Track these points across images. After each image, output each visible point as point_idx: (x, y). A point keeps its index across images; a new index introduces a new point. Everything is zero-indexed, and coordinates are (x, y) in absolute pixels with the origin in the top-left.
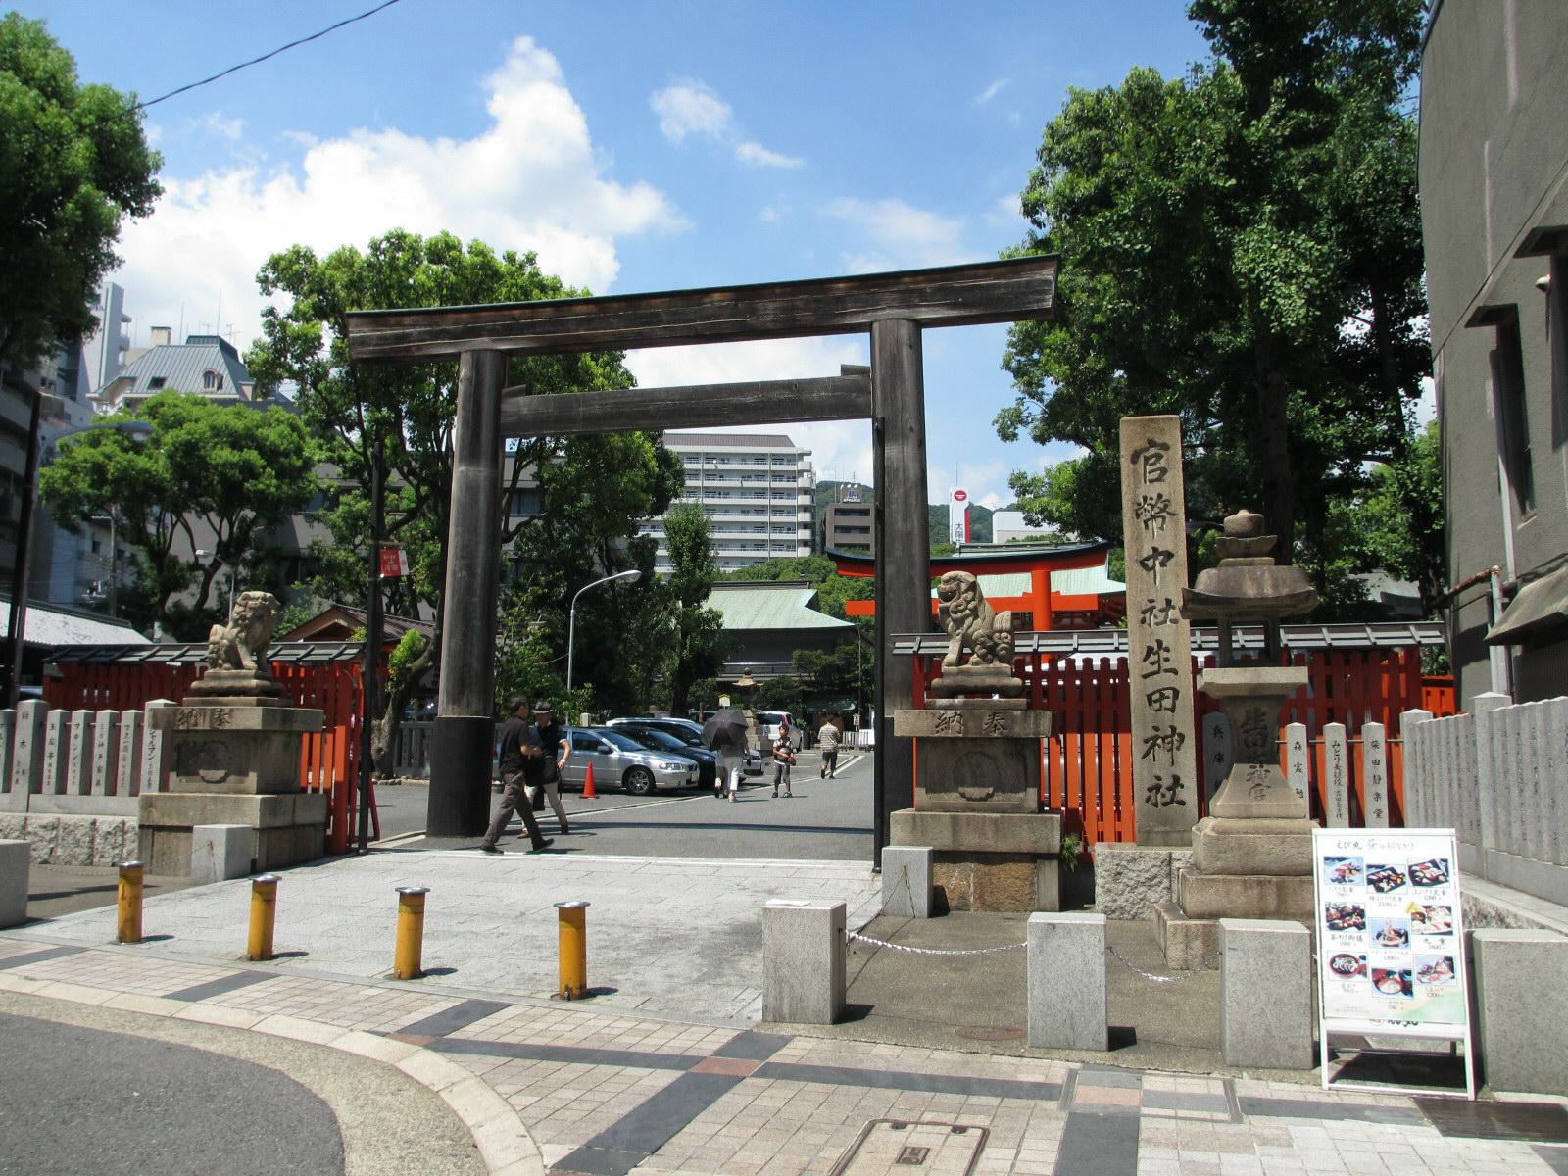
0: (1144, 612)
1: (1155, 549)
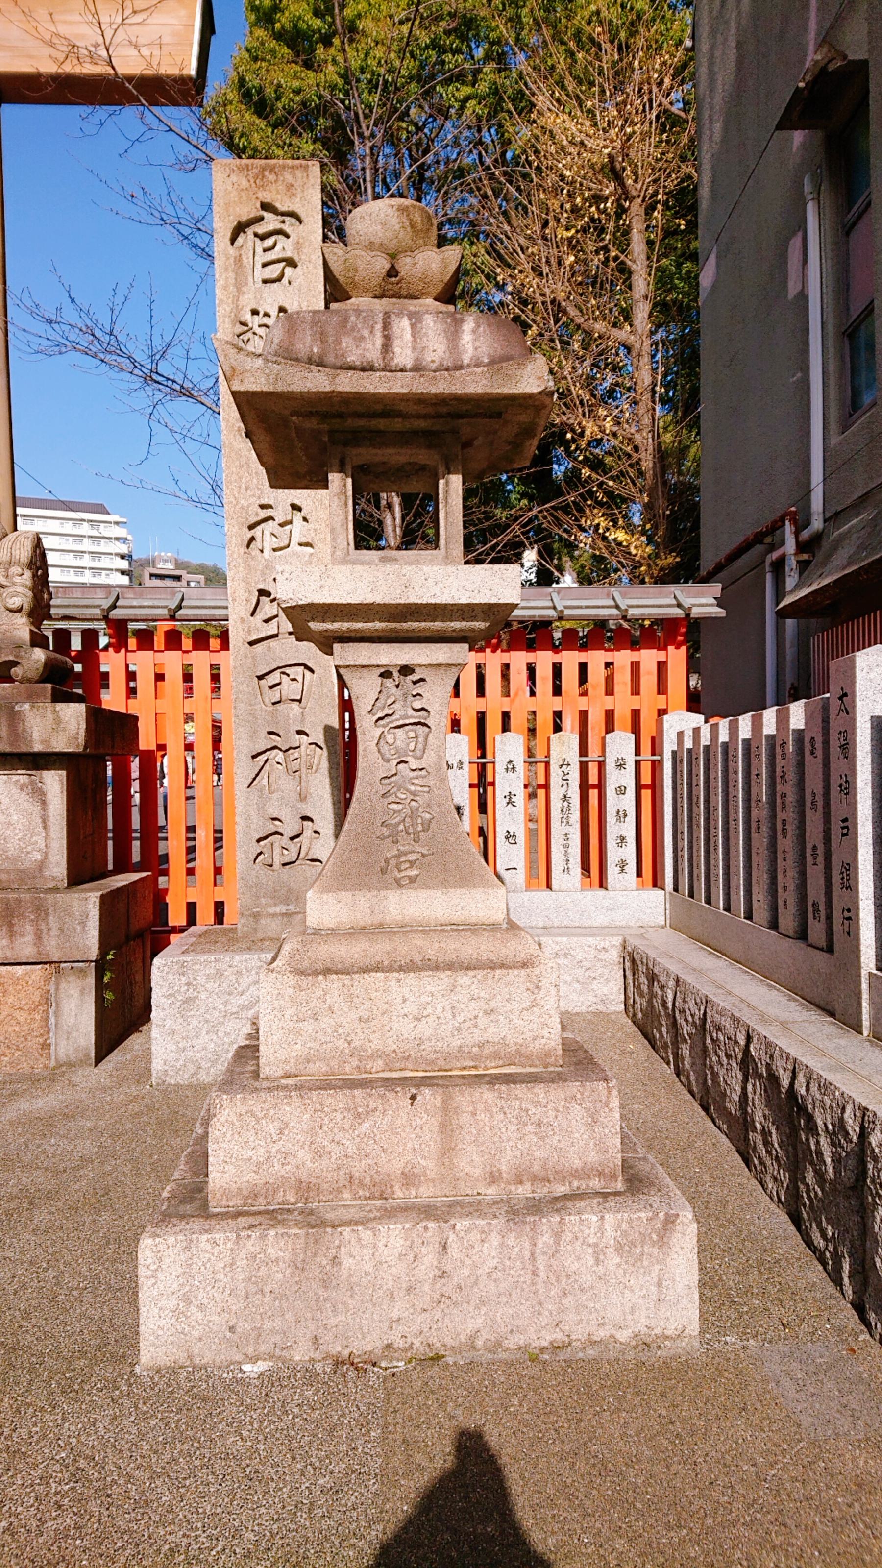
0: (251, 527)
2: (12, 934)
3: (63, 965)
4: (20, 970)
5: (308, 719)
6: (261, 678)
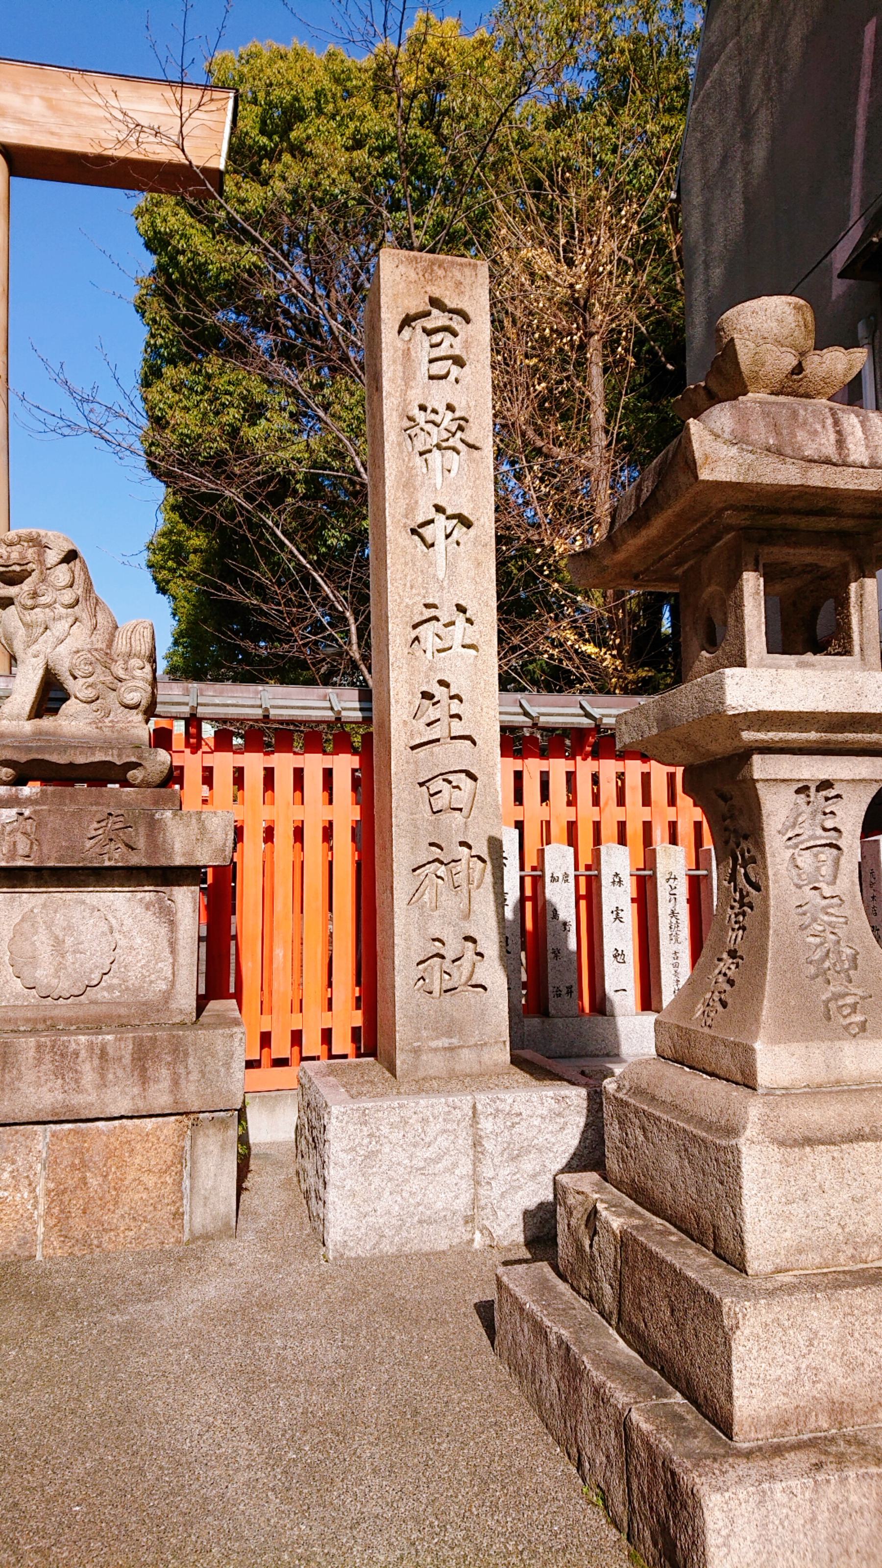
1: (439, 509)
2: (144, 1080)
3: (201, 1116)
4: (149, 1123)
5: (472, 829)
6: (421, 784)
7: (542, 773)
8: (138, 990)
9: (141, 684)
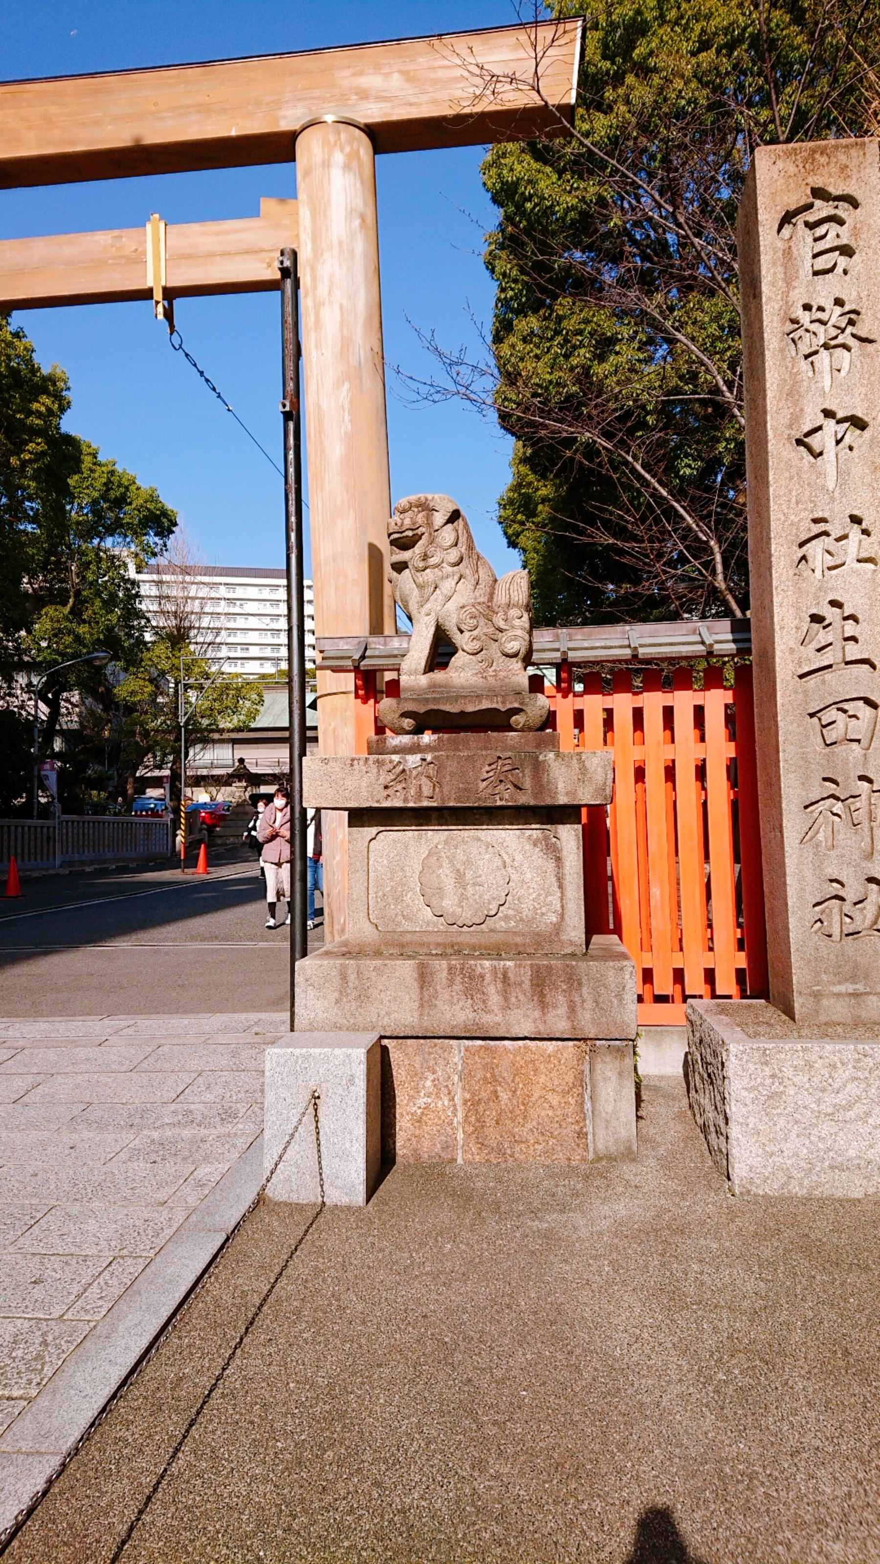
1: (828, 414)
2: (543, 1006)
3: (598, 1043)
4: (551, 1046)
5: (872, 762)
6: (812, 715)
7: (665, 708)
8: (529, 922)
9: (519, 632)
